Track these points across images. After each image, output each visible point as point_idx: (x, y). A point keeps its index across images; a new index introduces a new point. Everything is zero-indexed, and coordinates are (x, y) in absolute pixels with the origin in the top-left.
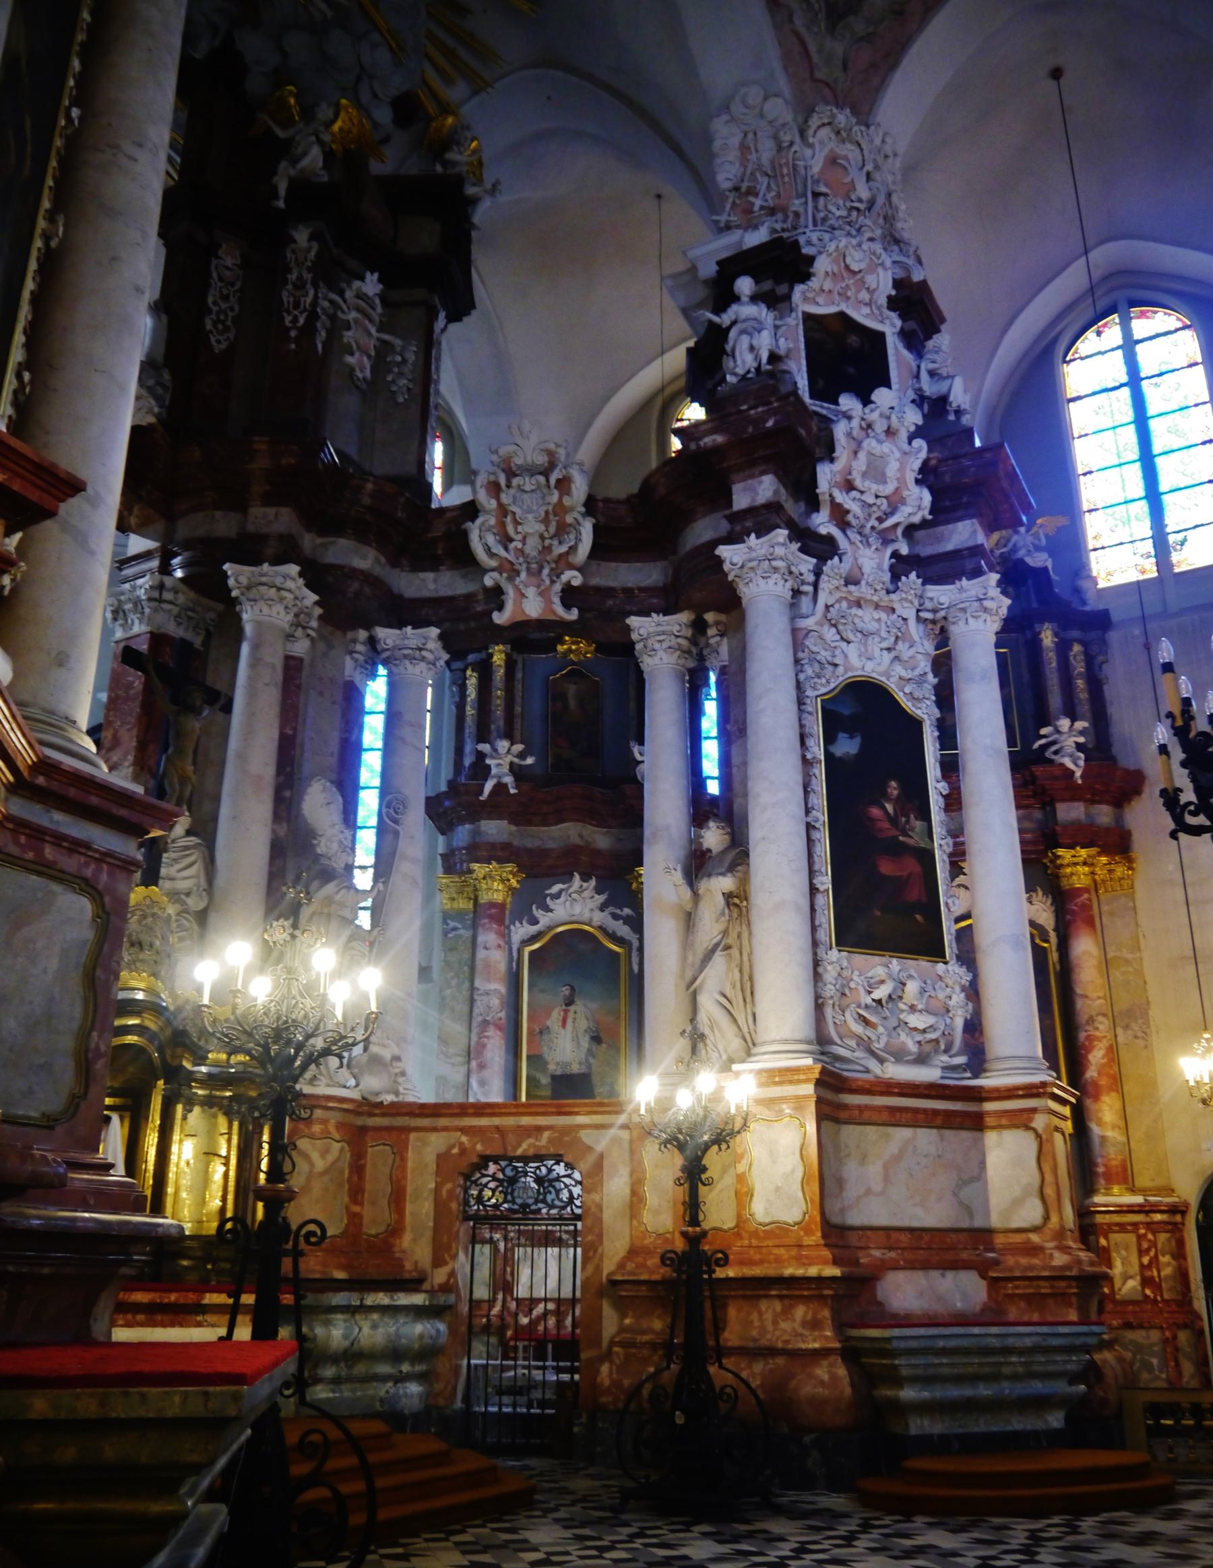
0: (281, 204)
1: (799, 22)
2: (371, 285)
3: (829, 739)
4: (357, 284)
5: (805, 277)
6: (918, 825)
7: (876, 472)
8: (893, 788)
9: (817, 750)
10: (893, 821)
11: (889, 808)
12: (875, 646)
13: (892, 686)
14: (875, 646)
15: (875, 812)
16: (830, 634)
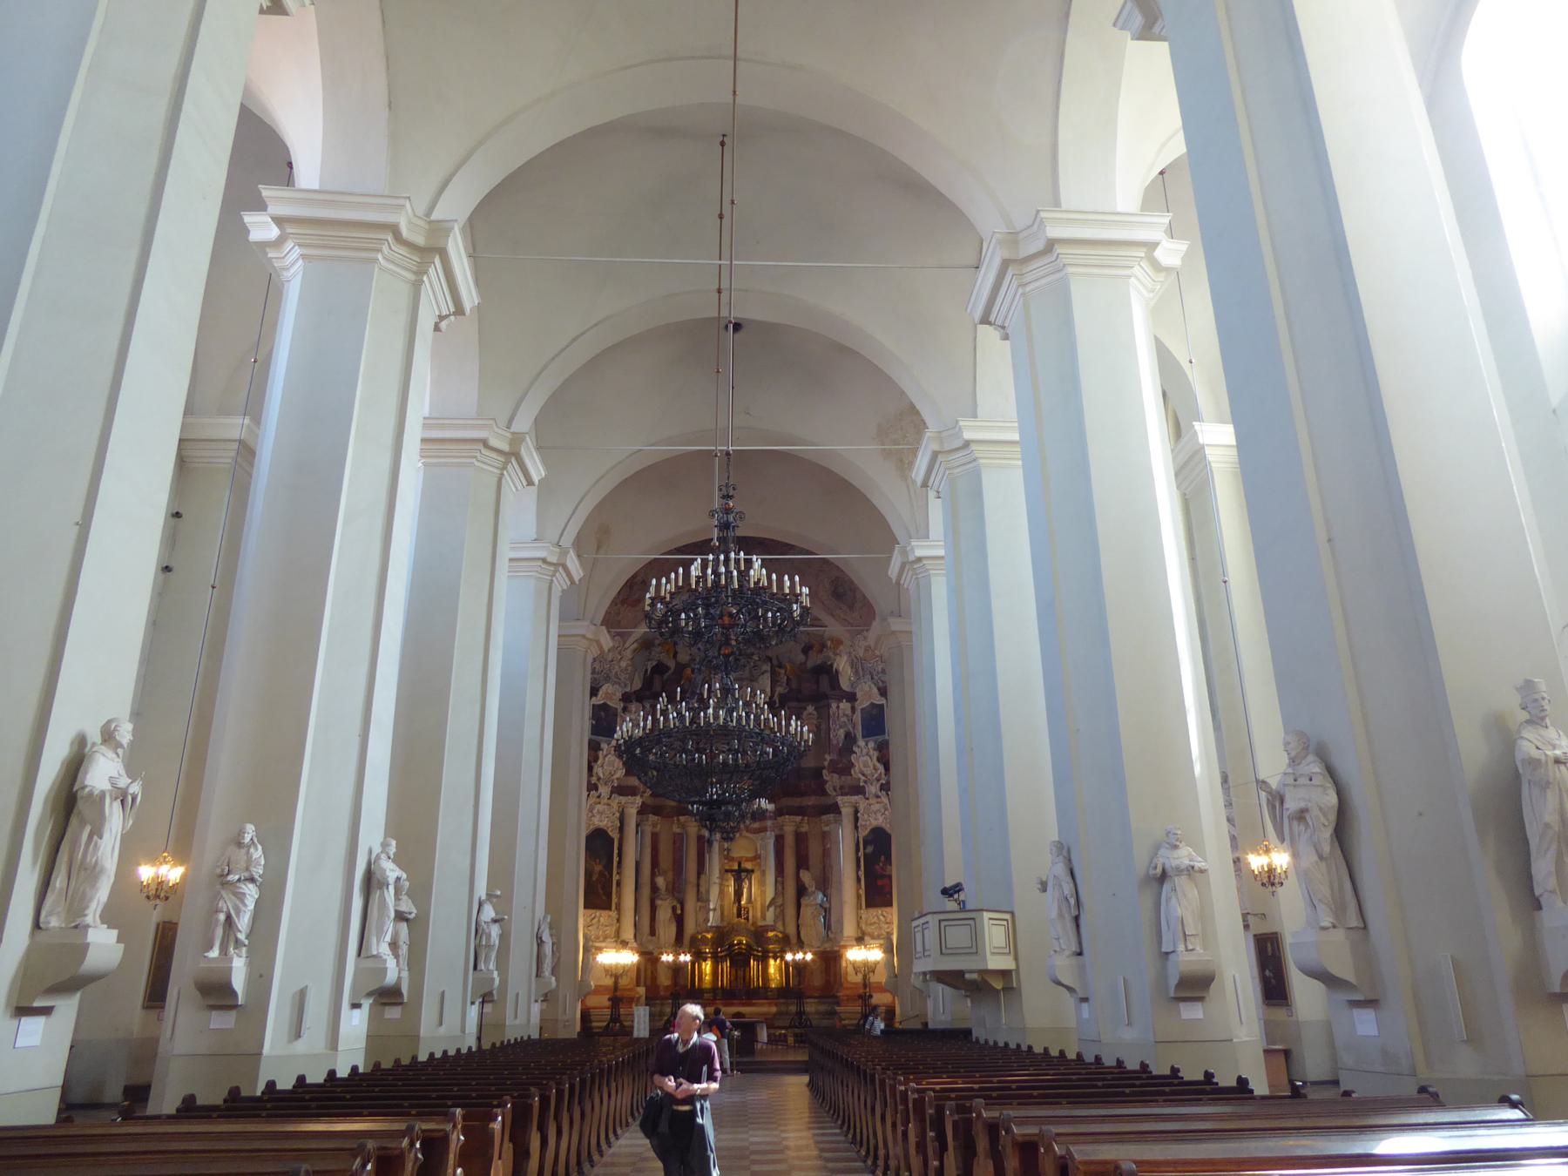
0: (777, 705)
1: (842, 615)
2: (810, 709)
3: (864, 848)
4: (805, 713)
5: (856, 700)
6: (889, 867)
7: (866, 765)
8: (883, 858)
9: (861, 853)
10: (882, 869)
11: (881, 865)
12: (879, 815)
13: (883, 825)
14: (879, 815)
15: (877, 867)
16: (866, 816)
